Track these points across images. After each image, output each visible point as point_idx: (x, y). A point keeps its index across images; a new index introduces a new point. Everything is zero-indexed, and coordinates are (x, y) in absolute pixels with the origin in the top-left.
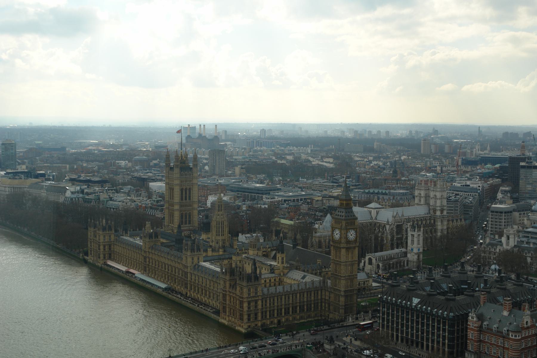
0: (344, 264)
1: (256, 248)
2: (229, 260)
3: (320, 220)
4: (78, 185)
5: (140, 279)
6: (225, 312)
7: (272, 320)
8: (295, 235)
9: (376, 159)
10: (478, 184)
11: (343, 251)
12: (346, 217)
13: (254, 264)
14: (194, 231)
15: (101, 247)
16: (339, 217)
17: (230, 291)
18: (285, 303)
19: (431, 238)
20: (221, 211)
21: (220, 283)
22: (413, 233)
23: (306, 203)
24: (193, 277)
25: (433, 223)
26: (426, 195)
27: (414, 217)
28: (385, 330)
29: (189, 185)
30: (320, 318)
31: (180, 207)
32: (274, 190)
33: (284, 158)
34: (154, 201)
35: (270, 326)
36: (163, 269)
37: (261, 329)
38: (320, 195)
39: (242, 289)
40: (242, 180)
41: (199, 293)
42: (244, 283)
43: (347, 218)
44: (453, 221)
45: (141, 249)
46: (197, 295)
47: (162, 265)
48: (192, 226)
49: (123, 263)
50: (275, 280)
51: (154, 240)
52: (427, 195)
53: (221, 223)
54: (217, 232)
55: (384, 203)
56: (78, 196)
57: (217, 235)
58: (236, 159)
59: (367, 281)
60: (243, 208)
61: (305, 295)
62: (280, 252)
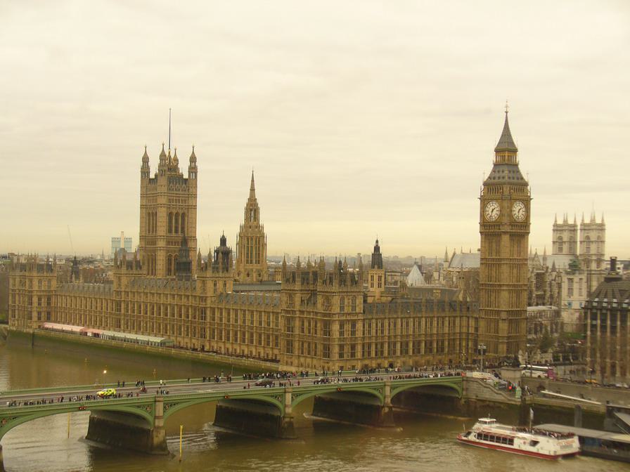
11: (506, 239)
12: (509, 178)
16: (496, 180)
18: (402, 333)
24: (217, 314)
26: (570, 239)
29: (182, 209)
31: (167, 245)
41: (228, 340)
42: (335, 287)
43: (512, 180)
54: (248, 257)
57: (247, 262)
61: (435, 323)
62: (376, 266)
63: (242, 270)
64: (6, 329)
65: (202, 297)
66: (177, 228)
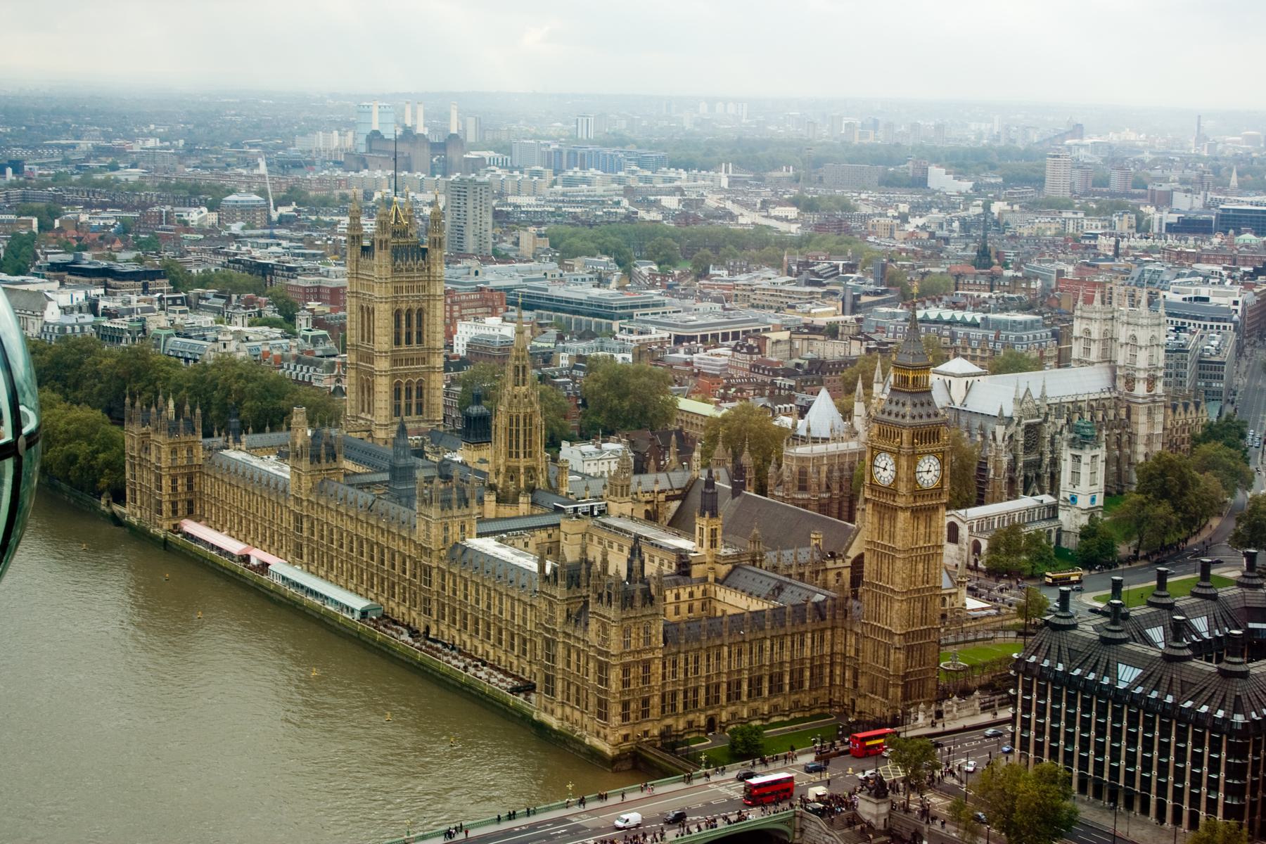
0: (906, 555)
1: (627, 495)
2: (550, 532)
3: (790, 399)
4: (78, 286)
5: (284, 578)
6: (550, 691)
7: (691, 717)
8: (736, 456)
9: (918, 209)
10: (1234, 294)
12: (914, 418)
13: (636, 551)
14: (435, 437)
15: (163, 482)
16: (892, 418)
17: (569, 631)
18: (729, 667)
19: (1118, 460)
20: (524, 385)
21: (531, 605)
22: (1078, 453)
23: (745, 350)
25: (1124, 417)
26: (1105, 334)
27: (1070, 399)
28: (1031, 755)
29: (418, 301)
30: (827, 711)
32: (645, 306)
33: (656, 204)
34: (305, 338)
35: (687, 737)
36: (354, 555)
37: (659, 744)
38: (777, 322)
39: (604, 627)
40: (545, 274)
42: (612, 612)
44: (1174, 408)
45: (285, 491)
46: (460, 636)
47: (352, 542)
48: (428, 421)
49: (230, 529)
50: (691, 594)
51: (324, 465)
52: (1109, 336)
53: (525, 420)
55: (969, 352)
56: (81, 321)
57: (511, 456)
58: (516, 206)
59: (950, 595)
60: (561, 362)
62: (707, 514)
63: (502, 469)
64: (123, 515)
65: (426, 548)
66: (409, 335)
